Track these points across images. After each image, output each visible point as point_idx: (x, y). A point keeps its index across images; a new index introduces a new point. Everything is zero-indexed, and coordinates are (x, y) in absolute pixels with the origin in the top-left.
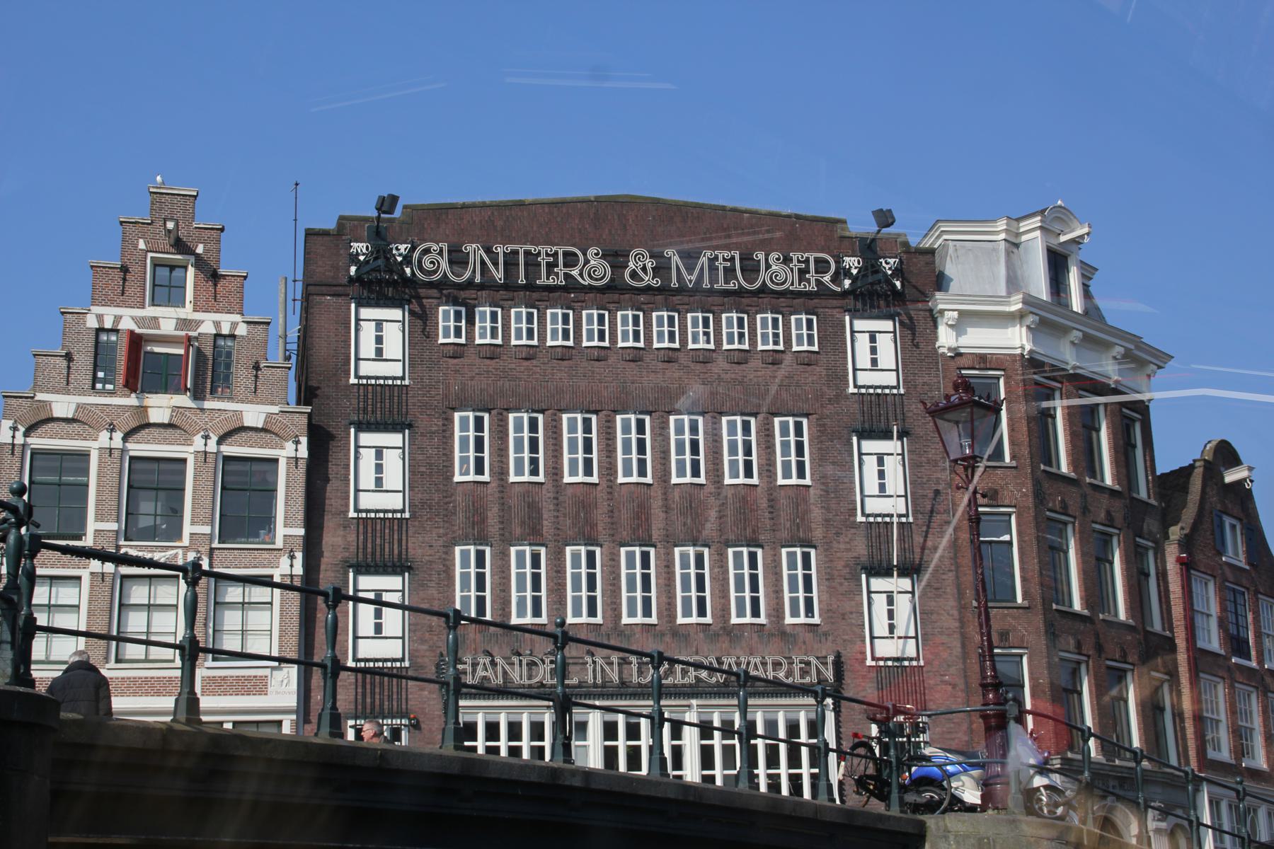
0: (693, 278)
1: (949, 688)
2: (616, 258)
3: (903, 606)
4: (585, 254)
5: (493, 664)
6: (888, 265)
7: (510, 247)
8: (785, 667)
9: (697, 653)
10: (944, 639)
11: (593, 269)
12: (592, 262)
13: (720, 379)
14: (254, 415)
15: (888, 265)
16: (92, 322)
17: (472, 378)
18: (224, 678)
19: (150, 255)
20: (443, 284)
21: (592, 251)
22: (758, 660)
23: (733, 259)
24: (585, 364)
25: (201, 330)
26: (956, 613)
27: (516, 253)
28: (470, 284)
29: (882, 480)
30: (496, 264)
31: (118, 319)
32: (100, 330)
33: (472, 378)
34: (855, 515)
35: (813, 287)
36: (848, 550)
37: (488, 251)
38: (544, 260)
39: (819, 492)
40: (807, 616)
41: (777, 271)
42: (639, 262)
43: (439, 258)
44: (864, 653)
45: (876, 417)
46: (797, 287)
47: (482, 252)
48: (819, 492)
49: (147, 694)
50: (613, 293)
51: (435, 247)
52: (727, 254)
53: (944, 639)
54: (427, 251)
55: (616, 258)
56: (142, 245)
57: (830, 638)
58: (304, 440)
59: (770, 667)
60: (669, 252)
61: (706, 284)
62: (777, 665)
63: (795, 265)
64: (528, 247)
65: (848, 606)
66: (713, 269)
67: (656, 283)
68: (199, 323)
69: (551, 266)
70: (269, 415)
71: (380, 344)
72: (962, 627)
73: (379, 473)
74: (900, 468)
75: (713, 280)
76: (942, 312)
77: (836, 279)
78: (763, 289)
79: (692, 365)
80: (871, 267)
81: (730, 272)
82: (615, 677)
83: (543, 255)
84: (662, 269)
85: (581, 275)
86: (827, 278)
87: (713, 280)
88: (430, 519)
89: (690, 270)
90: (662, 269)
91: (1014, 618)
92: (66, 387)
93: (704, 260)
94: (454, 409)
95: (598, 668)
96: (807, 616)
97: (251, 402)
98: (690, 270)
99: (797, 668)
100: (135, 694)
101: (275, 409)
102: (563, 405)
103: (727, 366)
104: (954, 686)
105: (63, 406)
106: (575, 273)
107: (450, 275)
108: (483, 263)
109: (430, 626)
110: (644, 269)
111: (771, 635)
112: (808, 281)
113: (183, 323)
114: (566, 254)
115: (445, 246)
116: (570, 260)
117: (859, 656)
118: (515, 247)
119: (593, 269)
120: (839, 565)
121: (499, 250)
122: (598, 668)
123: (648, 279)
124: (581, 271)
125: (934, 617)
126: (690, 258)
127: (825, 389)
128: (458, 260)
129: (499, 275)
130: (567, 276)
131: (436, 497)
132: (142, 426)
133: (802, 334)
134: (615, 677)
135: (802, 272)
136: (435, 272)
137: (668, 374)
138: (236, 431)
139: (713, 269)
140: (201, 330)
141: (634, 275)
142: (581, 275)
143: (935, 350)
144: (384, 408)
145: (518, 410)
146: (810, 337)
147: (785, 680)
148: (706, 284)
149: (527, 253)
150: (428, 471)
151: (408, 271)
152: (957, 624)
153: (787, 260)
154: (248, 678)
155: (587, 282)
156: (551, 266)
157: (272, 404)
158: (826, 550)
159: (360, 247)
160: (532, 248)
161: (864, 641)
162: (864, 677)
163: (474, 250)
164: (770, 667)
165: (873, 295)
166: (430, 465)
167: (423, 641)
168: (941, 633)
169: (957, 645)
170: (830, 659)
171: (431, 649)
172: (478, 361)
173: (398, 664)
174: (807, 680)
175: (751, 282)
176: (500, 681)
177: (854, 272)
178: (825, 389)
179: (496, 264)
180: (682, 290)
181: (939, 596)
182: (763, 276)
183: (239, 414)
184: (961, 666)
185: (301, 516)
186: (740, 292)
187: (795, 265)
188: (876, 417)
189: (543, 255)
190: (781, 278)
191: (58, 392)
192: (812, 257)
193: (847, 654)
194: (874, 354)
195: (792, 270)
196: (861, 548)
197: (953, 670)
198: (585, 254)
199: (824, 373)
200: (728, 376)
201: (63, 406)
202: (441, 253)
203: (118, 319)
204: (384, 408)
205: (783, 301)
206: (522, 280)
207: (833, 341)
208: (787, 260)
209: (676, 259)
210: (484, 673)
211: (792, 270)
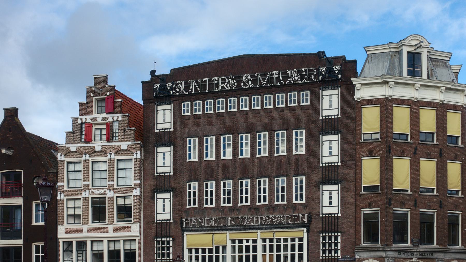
0: (265, 82)
1: (349, 223)
2: (239, 79)
3: (335, 196)
4: (228, 80)
5: (197, 220)
6: (337, 68)
7: (204, 79)
8: (290, 218)
9: (262, 214)
10: (349, 206)
11: (231, 83)
13: (274, 118)
14: (124, 146)
15: (337, 68)
16: (79, 121)
17: (192, 126)
18: (119, 227)
19: (94, 97)
20: (183, 95)
21: (231, 77)
22: (281, 216)
23: (279, 74)
24: (229, 118)
25: (108, 120)
26: (354, 197)
27: (205, 81)
28: (191, 94)
29: (331, 150)
30: (199, 86)
31: (86, 119)
32: (82, 123)
33: (192, 126)
35: (308, 81)
36: (317, 176)
37: (197, 82)
38: (214, 82)
39: (307, 156)
40: (300, 200)
41: (295, 76)
42: (247, 79)
47: (194, 82)
48: (307, 156)
49: (99, 232)
50: (239, 92)
51: (180, 82)
52: (277, 72)
53: (349, 206)
54: (178, 84)
55: (239, 79)
56: (92, 95)
57: (308, 208)
59: (285, 218)
60: (257, 74)
61: (269, 84)
62: (288, 217)
63: (302, 73)
64: (209, 79)
65: (315, 196)
66: (272, 78)
67: (252, 86)
68: (108, 118)
69: (217, 84)
70: (129, 145)
72: (355, 202)
73: (164, 161)
74: (337, 145)
75: (272, 82)
76: (355, 85)
77: (316, 77)
78: (290, 84)
79: (265, 114)
80: (330, 71)
81: (278, 79)
82: (234, 223)
83: (214, 80)
84: (254, 81)
85: (227, 86)
86: (313, 77)
87: (272, 82)
88: (179, 174)
89: (264, 81)
91: (376, 197)
93: (269, 76)
95: (229, 221)
96: (300, 200)
97: (123, 142)
98: (264, 80)
99: (295, 218)
100: (96, 232)
101: (130, 143)
102: (221, 133)
103: (277, 113)
104: (351, 222)
106: (225, 86)
107: (184, 91)
108: (195, 85)
109: (179, 209)
110: (248, 81)
111: (288, 207)
112: (306, 79)
113: (104, 119)
114: (222, 79)
115: (183, 82)
116: (223, 81)
117: (318, 213)
119: (231, 83)
120: (313, 182)
121: (200, 80)
122: (229, 221)
123: (250, 85)
124: (227, 85)
125: (346, 198)
126: (264, 75)
127: (311, 118)
129: (200, 90)
131: (181, 167)
133: (305, 99)
134: (234, 223)
136: (179, 92)
137: (256, 118)
139: (272, 78)
140: (108, 120)
141: (245, 84)
143: (354, 99)
144: (165, 139)
145: (206, 136)
146: (307, 100)
147: (290, 223)
148: (269, 84)
149: (209, 80)
150: (179, 158)
151: (171, 92)
152: (354, 201)
154: (125, 227)
155: (229, 88)
156: (217, 84)
157: (129, 142)
158: (308, 177)
159: (157, 86)
160: (210, 79)
162: (319, 221)
163: (192, 82)
164: (285, 218)
165: (329, 82)
166: (179, 157)
167: (177, 214)
168: (348, 204)
169: (353, 208)
170: (306, 215)
171: (179, 216)
172: (194, 120)
173: (168, 221)
174: (298, 222)
175: (285, 81)
176: (199, 225)
177: (323, 73)
178: (311, 118)
179: (199, 86)
180: (261, 87)
181: (348, 191)
182: (290, 79)
183: (120, 146)
184: (354, 215)
185: (138, 177)
186: (282, 85)
187: (302, 73)
189: (214, 80)
190: (296, 79)
191: (71, 144)
192: (308, 69)
193: (314, 212)
195: (300, 75)
197: (351, 217)
198: (228, 78)
199: (311, 112)
200: (277, 117)
202: (181, 85)
203: (86, 119)
204: (165, 139)
205: (299, 88)
206: (207, 91)
208: (299, 72)
209: (259, 77)
210: (194, 224)
211: (300, 75)
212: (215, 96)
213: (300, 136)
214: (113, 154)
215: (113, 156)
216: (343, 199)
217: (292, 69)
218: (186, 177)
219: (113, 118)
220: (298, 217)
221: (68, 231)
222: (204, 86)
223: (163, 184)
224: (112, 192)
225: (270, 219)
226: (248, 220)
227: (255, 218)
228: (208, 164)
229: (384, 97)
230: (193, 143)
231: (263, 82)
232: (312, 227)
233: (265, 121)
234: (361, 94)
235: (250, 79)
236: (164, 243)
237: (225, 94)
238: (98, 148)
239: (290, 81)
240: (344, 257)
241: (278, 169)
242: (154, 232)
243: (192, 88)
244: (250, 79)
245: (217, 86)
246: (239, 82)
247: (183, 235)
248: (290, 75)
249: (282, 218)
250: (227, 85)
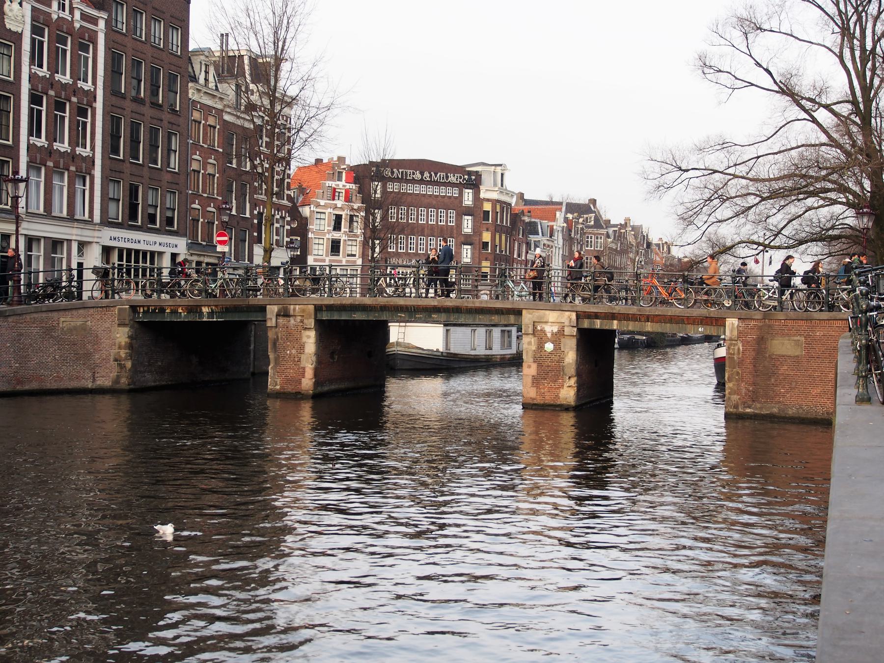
2: (422, 174)
11: (418, 176)
41: (452, 179)
42: (426, 174)
45: (468, 211)
50: (422, 182)
55: (422, 174)
71: (377, 190)
84: (431, 176)
90: (431, 176)
92: (323, 198)
105: (322, 202)
113: (344, 186)
116: (414, 174)
119: (418, 176)
123: (428, 179)
126: (436, 174)
128: (393, 173)
132: (335, 207)
133: (455, 192)
144: (378, 205)
150: (384, 217)
188: (468, 211)
194: (468, 198)
196: (463, 239)
201: (322, 202)
204: (378, 205)
205: (453, 185)
207: (461, 194)
212: (408, 181)
213: (452, 213)
216: (473, 254)
221: (315, 260)
230: (393, 211)
233: (434, 202)
234: (483, 195)
237: (414, 181)
238: (339, 206)
243: (395, 175)
246: (422, 175)
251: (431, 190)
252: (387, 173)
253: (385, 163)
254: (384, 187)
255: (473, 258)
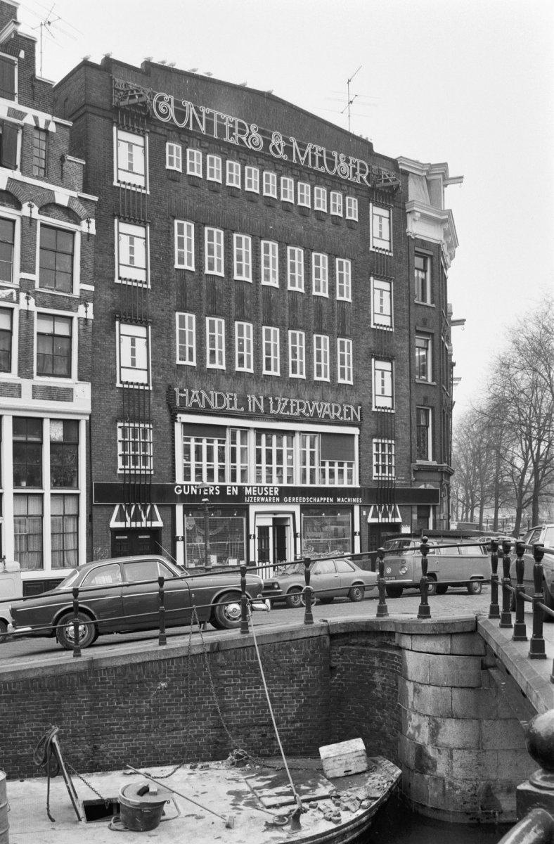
5: (200, 394)
7: (210, 110)
11: (254, 138)
12: (253, 134)
17: (185, 199)
20: (171, 127)
26: (408, 385)
34: (370, 324)
41: (344, 167)
43: (169, 106)
44: (371, 404)
46: (352, 179)
47: (193, 108)
54: (161, 99)
58: (93, 221)
60: (292, 139)
64: (221, 114)
65: (365, 376)
67: (285, 157)
78: (336, 177)
79: (299, 216)
81: (321, 164)
87: (313, 164)
89: (302, 156)
93: (308, 150)
94: (174, 218)
98: (302, 156)
101: (75, 194)
106: (244, 139)
109: (163, 364)
110: (279, 146)
118: (212, 111)
120: (362, 351)
121: (204, 110)
123: (282, 155)
124: (248, 137)
130: (241, 141)
135: (355, 170)
138: (49, 207)
139: (313, 156)
142: (247, 141)
143: (405, 234)
153: (347, 161)
155: (251, 147)
161: (371, 397)
167: (159, 374)
172: (189, 186)
175: (331, 169)
176: (203, 406)
182: (336, 168)
193: (365, 402)
202: (169, 103)
208: (347, 161)
209: (295, 145)
214: (36, 209)
215: (35, 214)
216: (396, 385)
217: (339, 153)
218: (173, 300)
219: (36, 119)
220: (349, 409)
222: (209, 124)
223: (125, 305)
224: (32, 301)
225: (313, 408)
226: (281, 406)
227: (292, 402)
228: (214, 285)
229: (436, 242)
231: (301, 158)
232: (365, 425)
235: (283, 144)
236: (140, 434)
239: (337, 173)
240: (399, 478)
241: (319, 319)
242: (115, 407)
244: (283, 144)
245: (231, 135)
247: (173, 420)
248: (336, 161)
249: (198, 396)
250: (248, 138)
251: (290, 191)
252: (165, 105)
253: (155, 73)
254: (156, 158)
255: (395, 397)
